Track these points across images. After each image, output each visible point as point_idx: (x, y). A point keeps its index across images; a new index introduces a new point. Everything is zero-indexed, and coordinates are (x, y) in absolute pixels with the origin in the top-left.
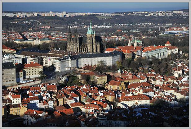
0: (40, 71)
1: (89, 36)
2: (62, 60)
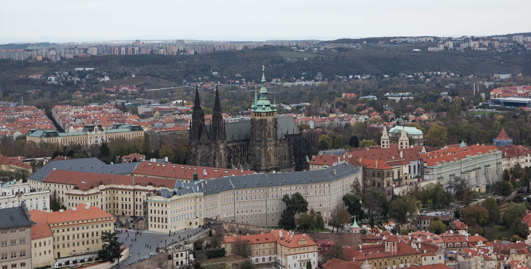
0: (106, 233)
1: (258, 118)
2: (175, 197)
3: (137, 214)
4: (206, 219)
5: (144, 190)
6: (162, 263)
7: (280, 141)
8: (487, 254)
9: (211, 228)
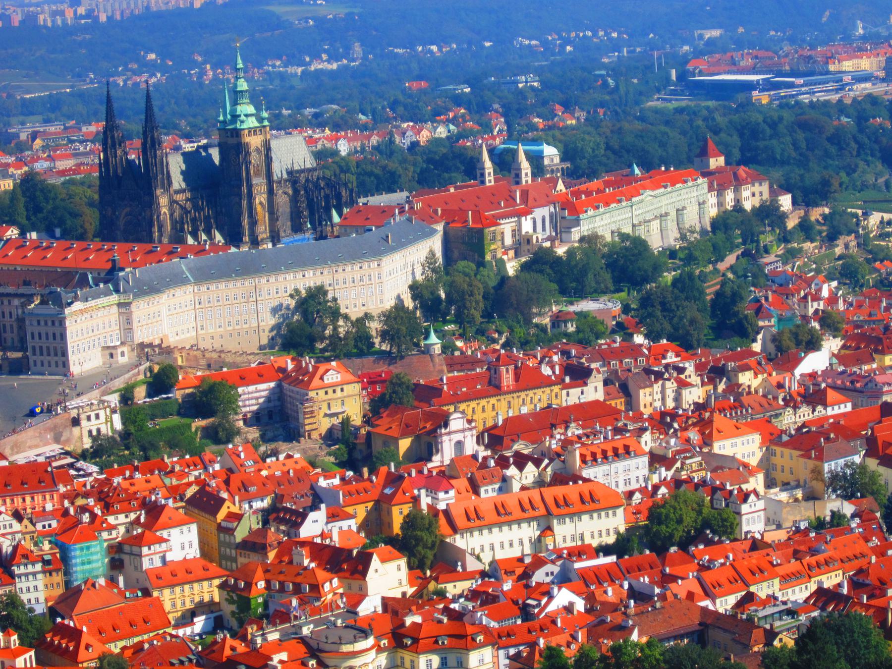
1: (232, 141)
2: (77, 306)
3: (5, 342)
4: (142, 346)
5: (16, 295)
6: (61, 434)
7: (279, 182)
8: (683, 376)
9: (151, 361)
